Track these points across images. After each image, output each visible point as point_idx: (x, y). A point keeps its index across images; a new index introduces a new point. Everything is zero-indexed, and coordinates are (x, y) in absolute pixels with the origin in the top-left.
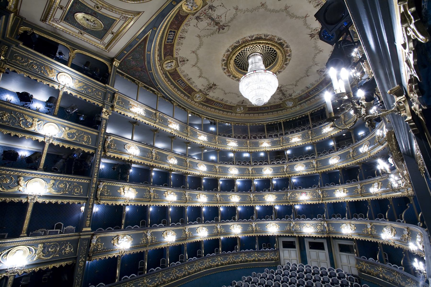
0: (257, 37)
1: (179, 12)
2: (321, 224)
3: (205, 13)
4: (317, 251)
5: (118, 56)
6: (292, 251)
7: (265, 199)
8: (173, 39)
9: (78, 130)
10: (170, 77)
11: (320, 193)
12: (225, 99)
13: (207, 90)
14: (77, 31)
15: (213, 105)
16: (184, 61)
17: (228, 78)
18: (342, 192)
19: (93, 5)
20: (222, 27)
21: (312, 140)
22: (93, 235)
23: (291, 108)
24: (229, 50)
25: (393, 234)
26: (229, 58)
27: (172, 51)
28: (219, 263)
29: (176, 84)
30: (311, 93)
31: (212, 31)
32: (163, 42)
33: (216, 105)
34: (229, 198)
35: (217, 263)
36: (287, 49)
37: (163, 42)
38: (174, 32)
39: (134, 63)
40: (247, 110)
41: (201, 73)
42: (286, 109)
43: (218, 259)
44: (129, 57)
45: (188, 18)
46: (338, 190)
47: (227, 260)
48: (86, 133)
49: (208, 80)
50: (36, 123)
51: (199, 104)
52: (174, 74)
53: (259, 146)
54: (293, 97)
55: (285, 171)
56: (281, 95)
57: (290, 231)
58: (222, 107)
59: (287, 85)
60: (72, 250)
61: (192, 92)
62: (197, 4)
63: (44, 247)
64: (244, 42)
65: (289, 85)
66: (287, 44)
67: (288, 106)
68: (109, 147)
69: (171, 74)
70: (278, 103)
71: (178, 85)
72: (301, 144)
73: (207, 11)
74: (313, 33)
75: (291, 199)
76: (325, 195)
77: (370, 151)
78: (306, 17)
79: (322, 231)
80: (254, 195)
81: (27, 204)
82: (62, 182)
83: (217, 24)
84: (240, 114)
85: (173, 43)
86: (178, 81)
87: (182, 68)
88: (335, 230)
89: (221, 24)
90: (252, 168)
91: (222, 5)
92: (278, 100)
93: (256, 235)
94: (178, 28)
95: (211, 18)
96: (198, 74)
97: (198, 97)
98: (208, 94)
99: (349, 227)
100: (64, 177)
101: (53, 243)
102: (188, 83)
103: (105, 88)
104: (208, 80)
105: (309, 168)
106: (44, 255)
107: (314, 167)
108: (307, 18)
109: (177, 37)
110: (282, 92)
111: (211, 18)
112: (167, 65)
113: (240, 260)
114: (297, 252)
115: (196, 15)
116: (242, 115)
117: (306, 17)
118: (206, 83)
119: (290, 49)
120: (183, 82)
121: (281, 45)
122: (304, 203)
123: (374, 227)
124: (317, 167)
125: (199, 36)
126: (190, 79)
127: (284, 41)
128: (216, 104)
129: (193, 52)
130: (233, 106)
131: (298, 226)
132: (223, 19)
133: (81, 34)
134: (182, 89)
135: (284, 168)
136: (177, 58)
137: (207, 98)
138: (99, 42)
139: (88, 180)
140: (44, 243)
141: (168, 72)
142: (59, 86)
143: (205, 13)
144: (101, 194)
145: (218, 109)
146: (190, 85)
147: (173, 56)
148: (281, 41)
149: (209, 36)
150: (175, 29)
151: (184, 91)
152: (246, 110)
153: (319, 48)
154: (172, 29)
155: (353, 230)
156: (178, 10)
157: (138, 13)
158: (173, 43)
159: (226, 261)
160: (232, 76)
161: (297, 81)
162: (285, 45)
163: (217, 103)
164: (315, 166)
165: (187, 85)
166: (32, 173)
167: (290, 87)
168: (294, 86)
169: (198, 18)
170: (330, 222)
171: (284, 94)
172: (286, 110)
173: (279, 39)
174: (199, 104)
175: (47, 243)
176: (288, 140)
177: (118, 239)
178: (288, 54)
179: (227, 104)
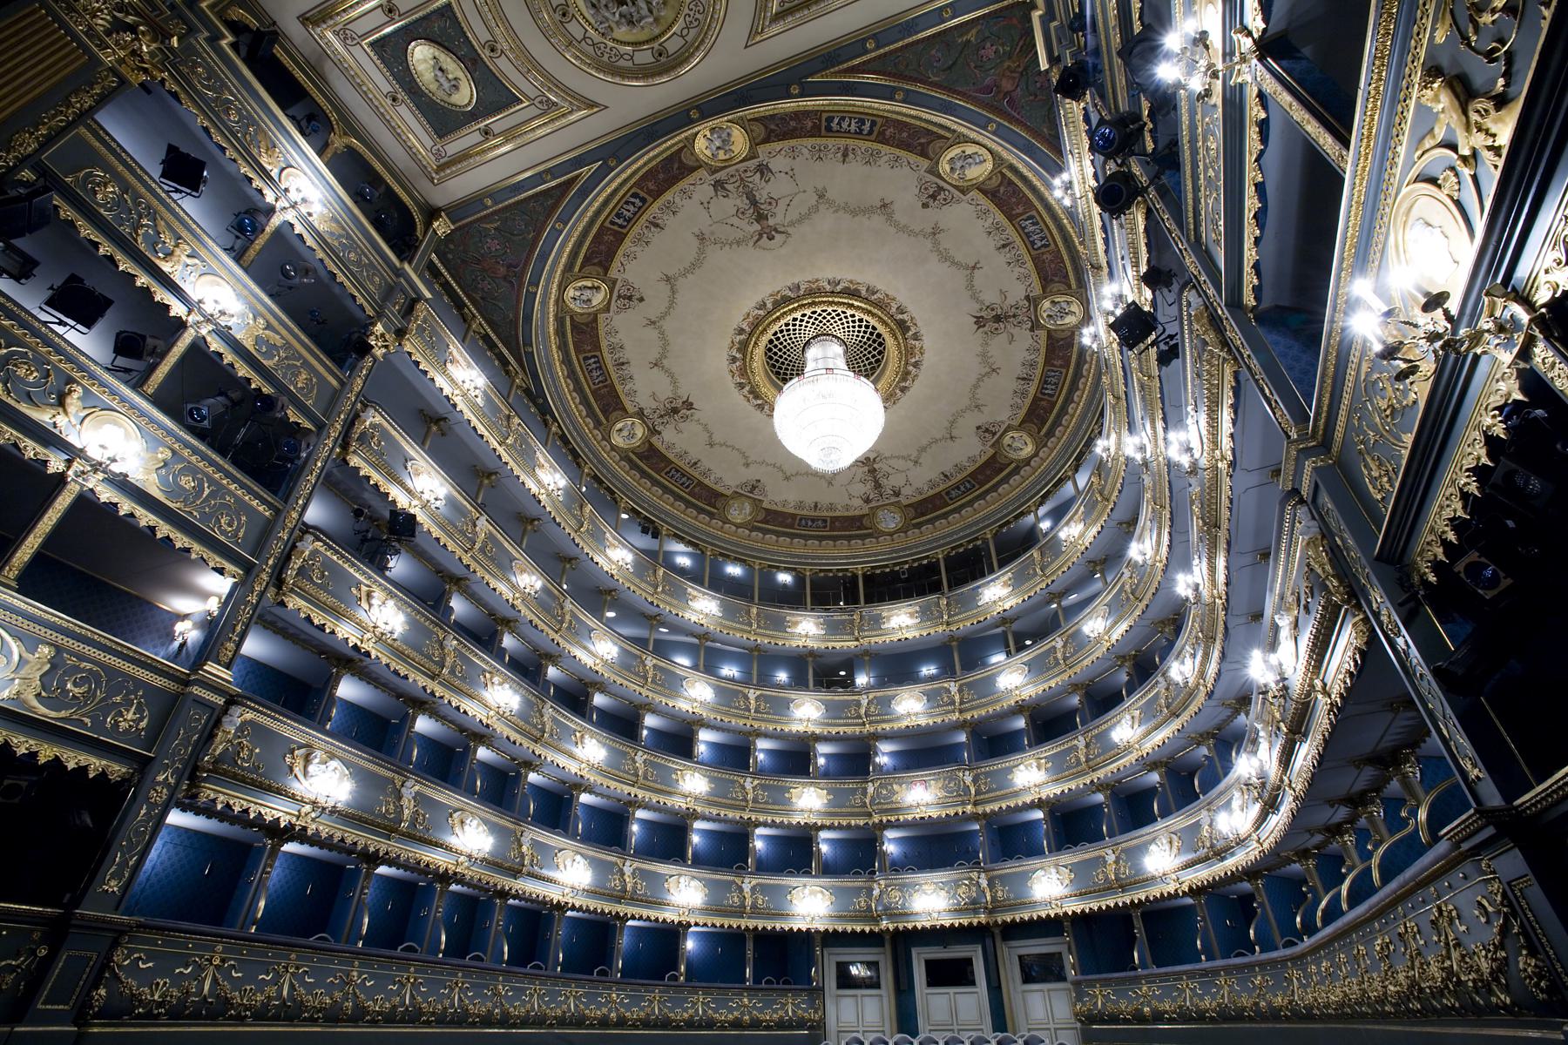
0: (848, 288)
1: (681, 150)
2: (971, 879)
3: (742, 179)
4: (952, 990)
5: (456, 211)
6: (866, 1000)
7: (794, 800)
8: (628, 222)
9: (287, 346)
10: (569, 335)
11: (968, 779)
12: (706, 463)
14: (386, 88)
16: (630, 298)
17: (735, 392)
18: (1035, 769)
19: (485, 36)
20: (770, 233)
21: (948, 624)
22: (232, 701)
23: (891, 534)
24: (765, 304)
25: (1175, 850)
26: (758, 325)
27: (610, 256)
28: (613, 1015)
29: (576, 362)
31: (740, 235)
32: (602, 217)
34: (674, 776)
35: (605, 1010)
37: (602, 217)
38: (643, 200)
39: (493, 245)
40: (761, 516)
41: (663, 356)
42: (877, 534)
43: (610, 995)
44: (491, 222)
45: (696, 175)
46: (1022, 767)
47: (642, 1009)
48: (306, 364)
49: (674, 382)
50: (182, 254)
51: (622, 459)
52: (583, 332)
53: (789, 630)
54: (901, 498)
55: (863, 711)
56: (870, 485)
57: (868, 916)
59: (892, 457)
60: (143, 724)
61: (615, 410)
62: (733, 148)
63: (55, 664)
64: (810, 293)
65: (898, 457)
67: (882, 527)
68: (363, 438)
69: (574, 326)
70: (857, 513)
72: (917, 634)
73: (749, 174)
74: (983, 314)
75: (879, 803)
76: (983, 787)
77: (1108, 631)
78: (974, 268)
79: (974, 902)
80: (756, 782)
81: (60, 480)
82: (191, 470)
83: (761, 217)
84: (738, 526)
85: (624, 231)
86: (586, 359)
87: (616, 318)
88: (1012, 896)
89: (771, 222)
90: (758, 693)
91: (791, 173)
92: (858, 502)
93: (751, 924)
94: (657, 194)
96: (654, 355)
97: (627, 434)
98: (659, 433)
99: (1054, 876)
100: (204, 457)
101: (89, 666)
102: (614, 376)
103: (399, 273)
104: (674, 382)
105: (938, 706)
106: (43, 694)
107: (953, 703)
109: (645, 217)
112: (578, 293)
113: (686, 1015)
114: (885, 1000)
115: (718, 176)
116: (740, 530)
117: (974, 268)
118: (665, 391)
120: (600, 368)
121: (903, 326)
122: (917, 816)
123: (1123, 856)
124: (962, 703)
125: (701, 238)
126: (623, 364)
128: (673, 472)
129: (668, 279)
130: (722, 495)
131: (898, 894)
133: (394, 100)
134: (588, 391)
135: (858, 704)
136: (614, 282)
137: (651, 445)
138: (429, 143)
139: (270, 506)
140: (59, 649)
141: (571, 317)
142: (277, 200)
143: (742, 179)
144: (301, 572)
145: (672, 493)
146: (616, 382)
147: (606, 270)
148: (905, 317)
149: (727, 247)
150: (649, 192)
151: (592, 400)
152: (759, 518)
153: (990, 360)
154: (642, 189)
155: (1067, 882)
156: (680, 145)
157: (591, 104)
158: (624, 231)
159: (634, 1013)
160: (747, 388)
161: (923, 449)
163: (677, 471)
164: (957, 698)
166: (113, 393)
167: (899, 464)
169: (719, 185)
170: (995, 873)
171: (878, 486)
172: (877, 538)
173: (901, 310)
174: (622, 459)
175: (72, 653)
176: (877, 621)
177: (307, 760)
179: (706, 481)
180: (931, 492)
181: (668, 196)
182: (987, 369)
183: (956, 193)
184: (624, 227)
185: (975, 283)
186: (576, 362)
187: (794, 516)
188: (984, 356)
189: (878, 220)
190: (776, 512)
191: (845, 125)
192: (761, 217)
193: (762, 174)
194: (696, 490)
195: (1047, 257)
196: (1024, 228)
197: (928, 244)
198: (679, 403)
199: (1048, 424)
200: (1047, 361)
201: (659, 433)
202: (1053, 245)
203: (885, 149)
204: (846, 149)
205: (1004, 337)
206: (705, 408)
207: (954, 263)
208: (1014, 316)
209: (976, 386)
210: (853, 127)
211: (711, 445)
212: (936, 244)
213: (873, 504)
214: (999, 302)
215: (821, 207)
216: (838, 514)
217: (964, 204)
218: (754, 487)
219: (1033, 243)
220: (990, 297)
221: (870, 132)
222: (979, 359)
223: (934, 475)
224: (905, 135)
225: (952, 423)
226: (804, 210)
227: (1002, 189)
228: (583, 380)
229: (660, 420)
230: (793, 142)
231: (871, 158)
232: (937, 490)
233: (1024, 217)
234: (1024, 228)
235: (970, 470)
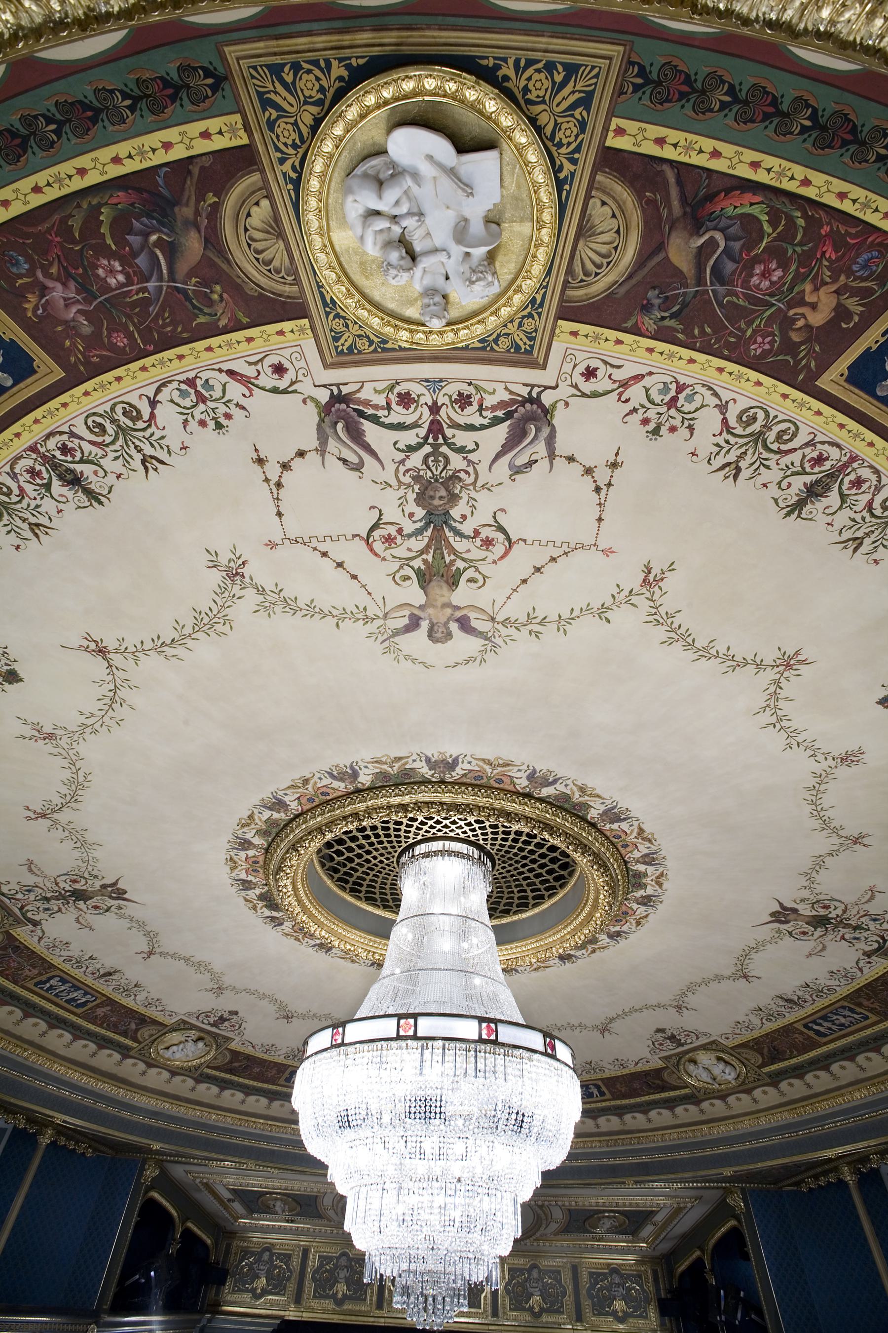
36: (250, 878)
65: (312, 610)
66: (243, 893)
110: (438, 542)
119: (232, 869)
127: (255, 908)
162: (253, 894)
178: (251, 853)
222: (90, 837)
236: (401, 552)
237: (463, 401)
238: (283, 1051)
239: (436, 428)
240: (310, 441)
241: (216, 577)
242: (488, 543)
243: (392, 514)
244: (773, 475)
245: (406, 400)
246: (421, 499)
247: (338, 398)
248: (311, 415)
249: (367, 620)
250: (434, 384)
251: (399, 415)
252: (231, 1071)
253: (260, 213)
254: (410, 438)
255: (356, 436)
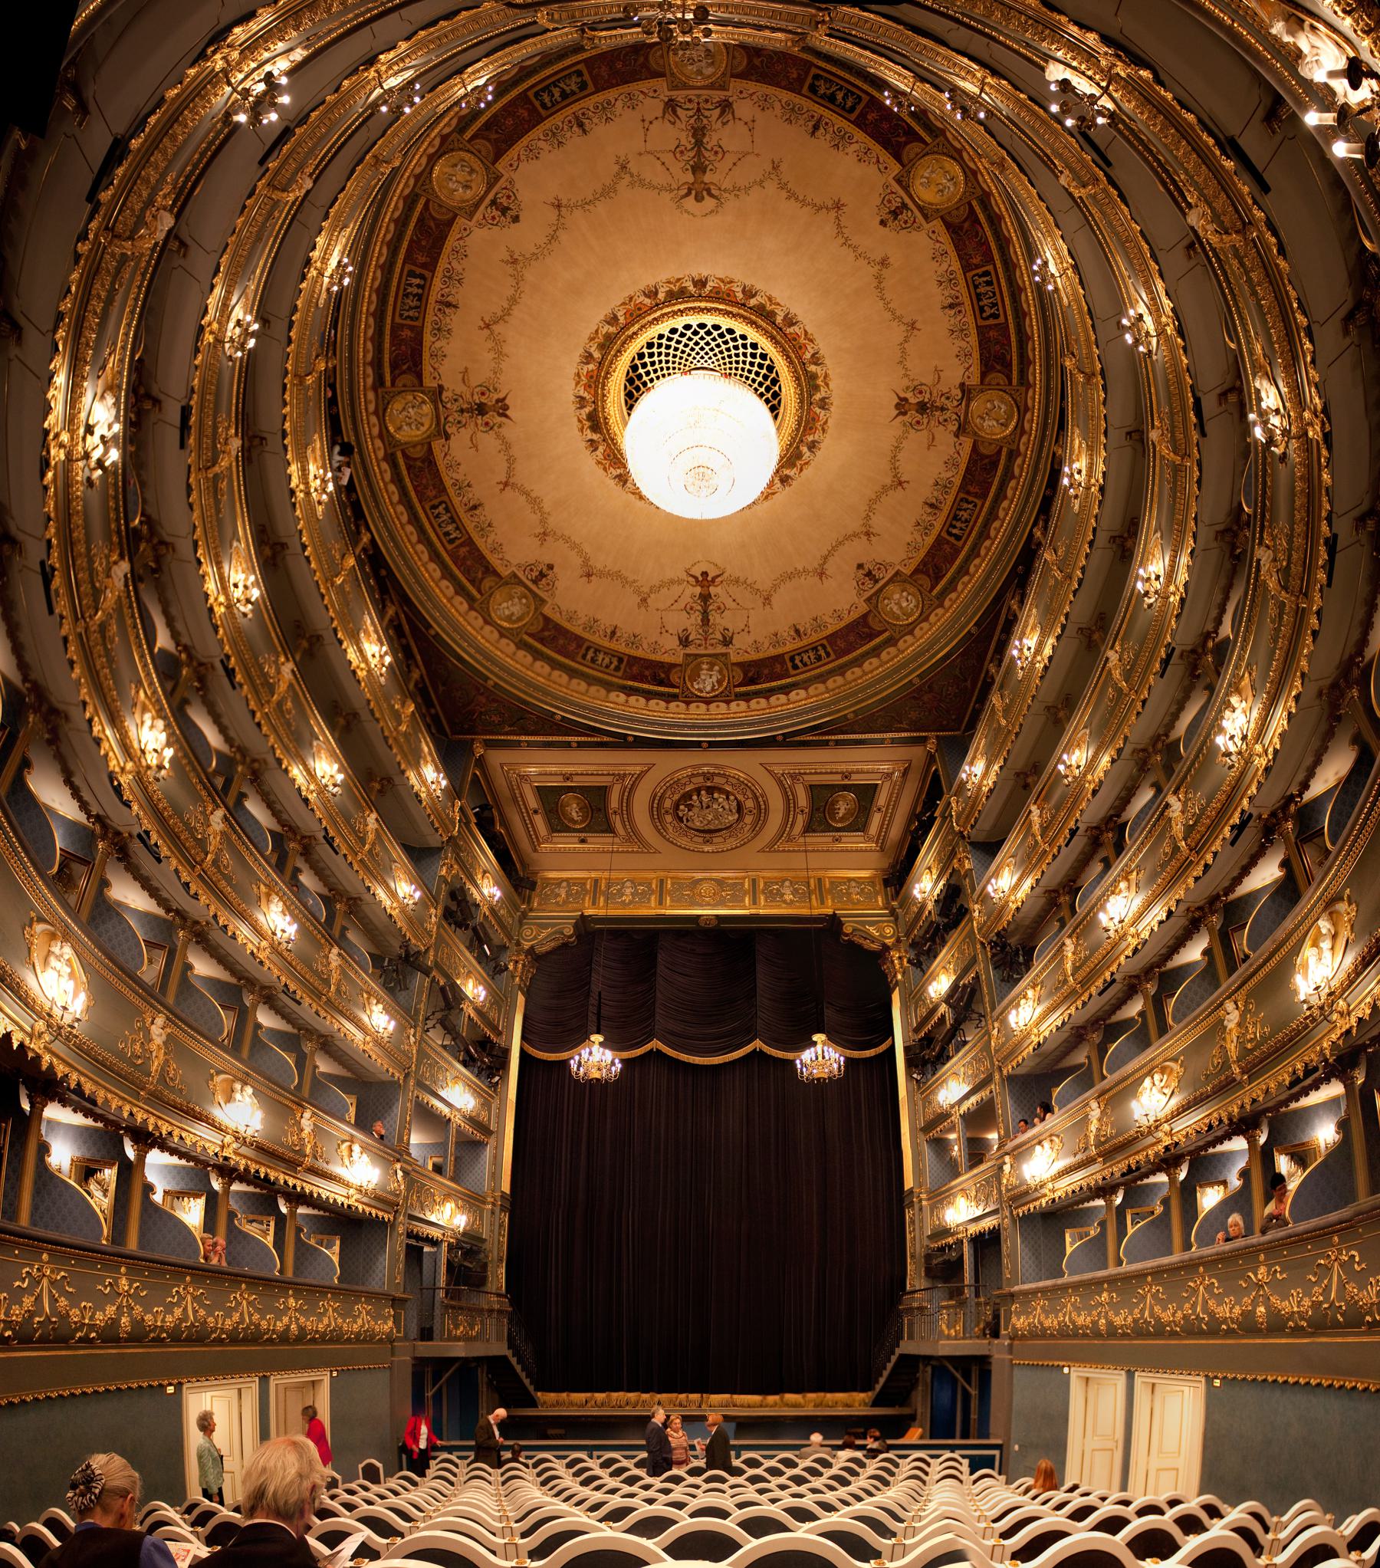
8: (815, 649)
10: (949, 575)
13: (943, 409)
15: (1002, 319)
16: (869, 574)
20: (705, 580)
27: (851, 627)
29: (969, 543)
30: (573, 85)
31: (733, 589)
33: (994, 305)
38: (792, 659)
54: (665, 94)
56: (711, 141)
58: (987, 274)
70: (752, 86)
71: (976, 528)
74: (499, 419)
78: (506, 484)
83: (705, 598)
85: (825, 642)
86: (958, 538)
89: (698, 590)
92: (744, 109)
95: (705, 621)
108: (504, 480)
109: (801, 644)
110: (699, 154)
111: (705, 621)
115: (724, 650)
117: (506, 484)
118: (917, 439)
125: (767, 601)
128: (988, 311)
129: (822, 574)
132: (686, 599)
137: (983, 375)
148: (590, 435)
150: (783, 663)
158: (825, 642)
163: (982, 310)
165: (962, 495)
167: (651, 171)
168: (632, 167)
171: (699, 134)
179: (956, 265)
180: (611, 94)
181: (773, 652)
182: (496, 328)
183: (520, 575)
184: (823, 646)
185: (506, 465)
186: (969, 543)
187: (860, 123)
188: (500, 355)
189: (599, 562)
190: (885, 144)
191: (607, 660)
192: (705, 598)
193: (687, 638)
194: (976, 261)
195: (431, 493)
196: (457, 528)
197: (552, 522)
198: (913, 415)
199: (414, 219)
200: (419, 341)
201: (962, 385)
202: (427, 508)
203: (578, 631)
204: (611, 637)
205: (474, 383)
206: (884, 389)
207: (527, 494)
208: (462, 411)
209: (513, 301)
210: (601, 656)
211: (912, 326)
212: (543, 521)
213: (717, 95)
214: (479, 435)
215: (646, 589)
216: (786, 96)
217: (514, 562)
218: (895, 214)
219: (447, 510)
220: (488, 441)
221: (588, 648)
223: (600, 130)
224: (561, 642)
225: (553, 238)
226: (664, 591)
227: (480, 575)
228: (980, 520)
229: (949, 404)
230: (653, 657)
231: (592, 624)
232: (599, 98)
233: (457, 542)
234: (457, 528)
235: (538, 132)
236: (685, 158)
237: (707, 101)
238: (584, 620)
239: (699, 110)
240: (660, 114)
241: (617, 168)
242: (716, 153)
243: (684, 142)
244: (801, 122)
245: (690, 101)
246: (694, 136)
247: (671, 100)
248: (662, 105)
249: (671, 191)
250: (699, 96)
251: (688, 106)
252: (542, 641)
253: (659, 53)
254: (691, 113)
255: (674, 112)
